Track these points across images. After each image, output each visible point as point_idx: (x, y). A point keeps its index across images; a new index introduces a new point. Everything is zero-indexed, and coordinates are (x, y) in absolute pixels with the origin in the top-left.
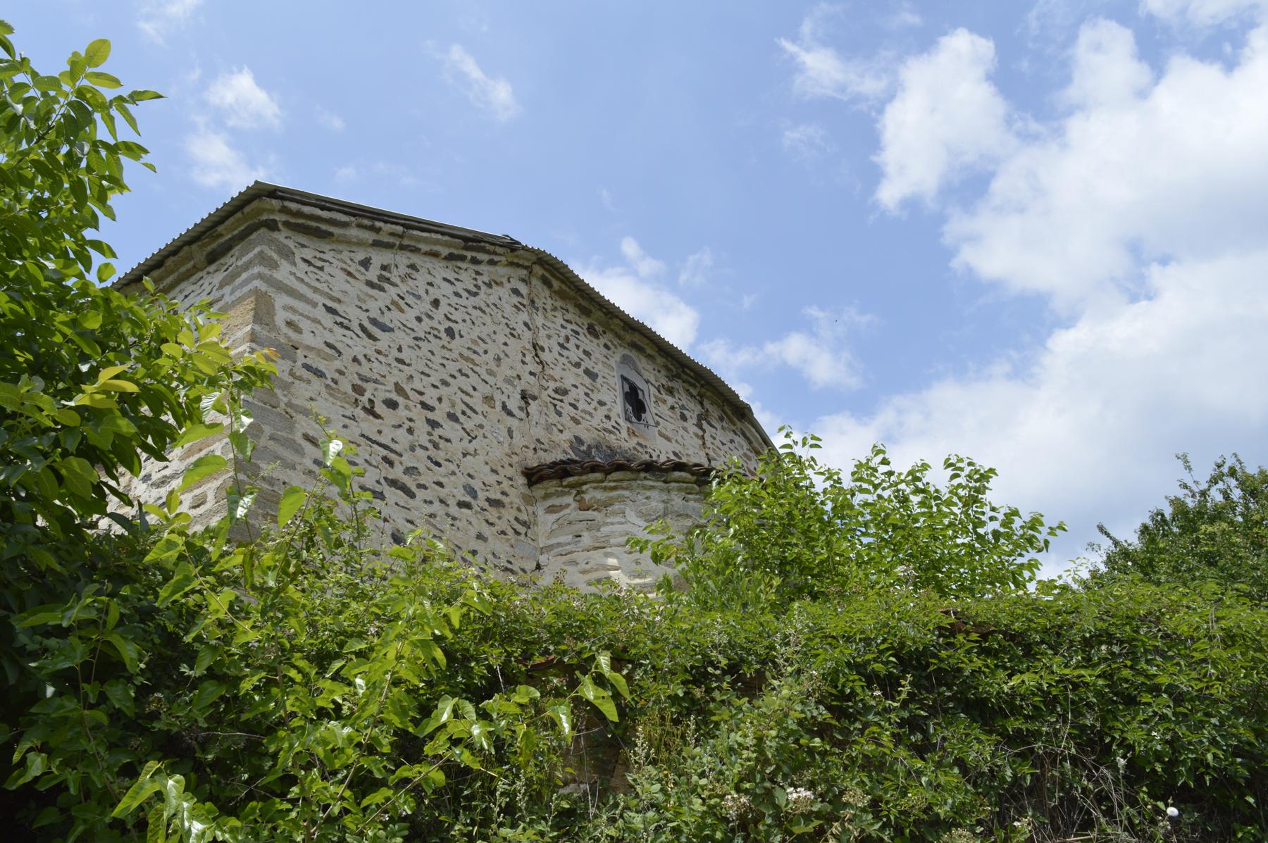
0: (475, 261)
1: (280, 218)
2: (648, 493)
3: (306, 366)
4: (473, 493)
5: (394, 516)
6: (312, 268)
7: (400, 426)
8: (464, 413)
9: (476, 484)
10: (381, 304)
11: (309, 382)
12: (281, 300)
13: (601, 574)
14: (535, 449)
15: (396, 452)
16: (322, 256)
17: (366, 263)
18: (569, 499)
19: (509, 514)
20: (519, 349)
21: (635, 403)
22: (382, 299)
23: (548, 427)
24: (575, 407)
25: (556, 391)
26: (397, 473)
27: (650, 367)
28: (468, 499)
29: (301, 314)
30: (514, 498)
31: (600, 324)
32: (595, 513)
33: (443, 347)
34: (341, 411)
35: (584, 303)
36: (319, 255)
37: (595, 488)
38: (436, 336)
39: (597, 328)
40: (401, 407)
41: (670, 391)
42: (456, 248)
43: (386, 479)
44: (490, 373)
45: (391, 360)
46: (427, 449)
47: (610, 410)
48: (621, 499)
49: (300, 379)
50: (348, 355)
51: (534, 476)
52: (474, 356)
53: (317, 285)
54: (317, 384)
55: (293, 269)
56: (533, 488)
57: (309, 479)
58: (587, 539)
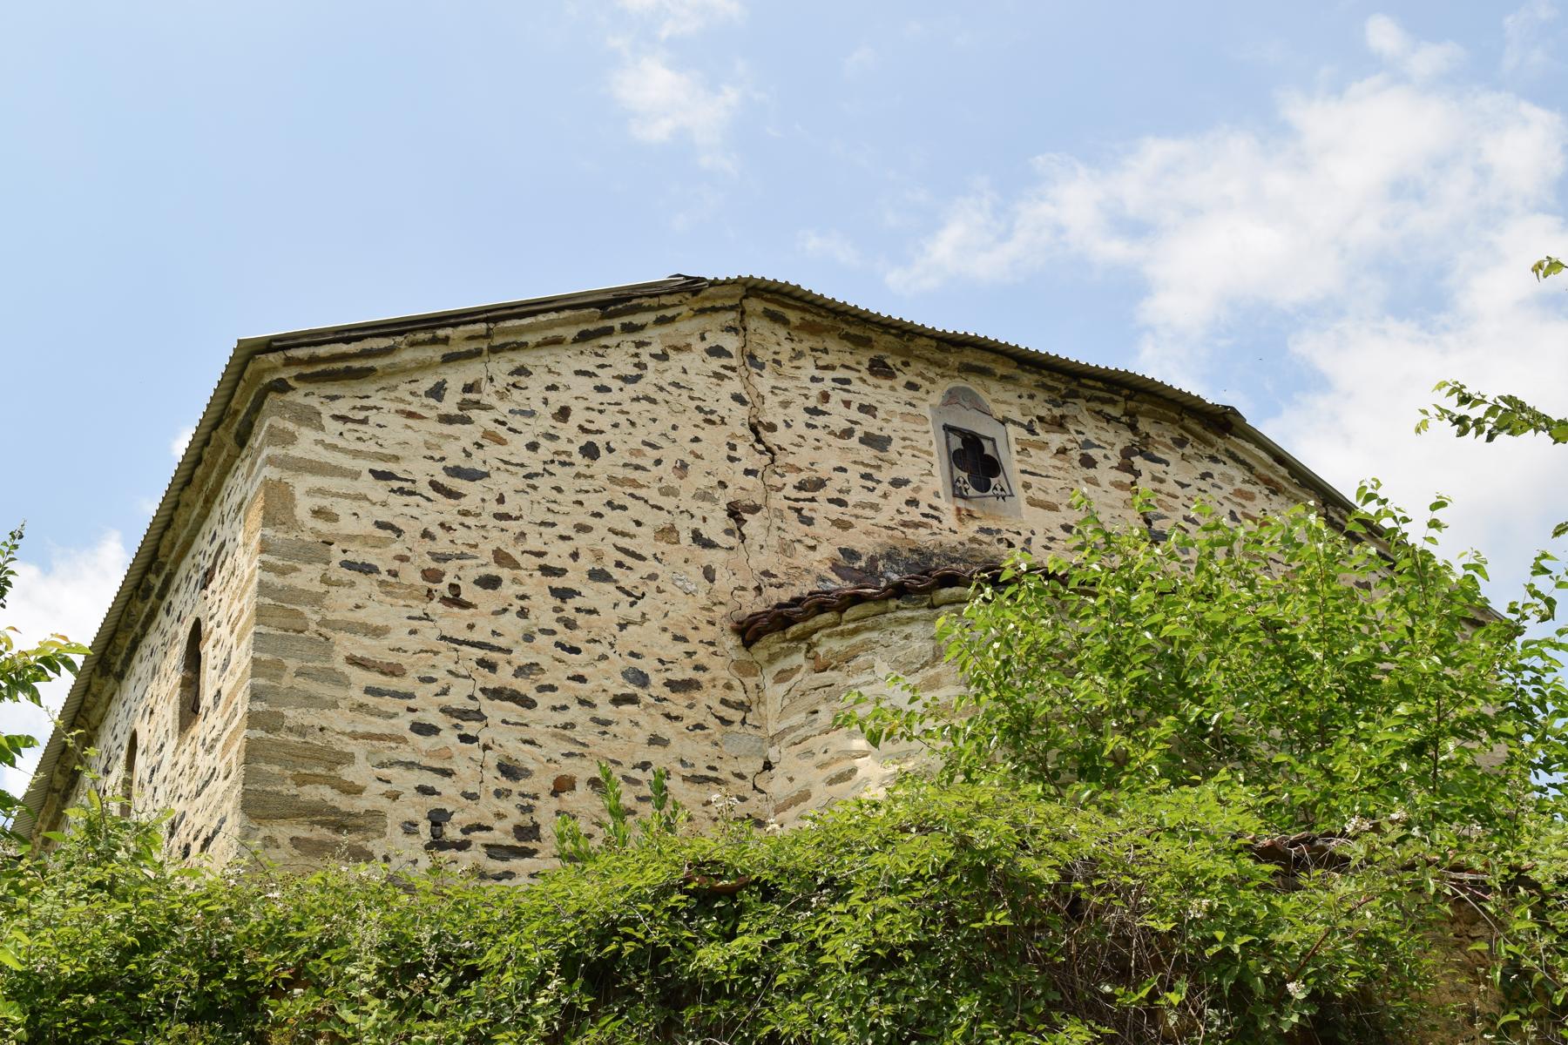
0: (629, 329)
1: (287, 374)
2: (907, 630)
3: (348, 565)
4: (642, 679)
5: (500, 739)
6: (350, 425)
7: (505, 610)
8: (619, 564)
9: (647, 665)
10: (467, 443)
11: (352, 584)
12: (301, 484)
13: (844, 766)
14: (758, 589)
15: (500, 649)
16: (365, 402)
17: (437, 392)
18: (799, 659)
19: (708, 698)
20: (723, 439)
21: (975, 463)
22: (467, 435)
23: (786, 548)
24: (841, 503)
25: (801, 487)
26: (504, 677)
27: (1011, 396)
28: (631, 689)
29: (337, 495)
30: (720, 670)
31: (894, 352)
32: (834, 674)
33: (578, 475)
34: (406, 612)
35: (853, 331)
36: (359, 403)
37: (829, 636)
38: (563, 464)
39: (889, 362)
40: (506, 582)
41: (1059, 424)
42: (588, 320)
43: (483, 690)
44: (668, 492)
45: (488, 519)
46: (553, 632)
47: (917, 489)
48: (867, 646)
49: (339, 584)
50: (412, 531)
51: (750, 631)
52: (637, 475)
53: (360, 446)
54: (364, 583)
55: (320, 436)
56: (752, 649)
57: (358, 716)
58: (825, 718)
